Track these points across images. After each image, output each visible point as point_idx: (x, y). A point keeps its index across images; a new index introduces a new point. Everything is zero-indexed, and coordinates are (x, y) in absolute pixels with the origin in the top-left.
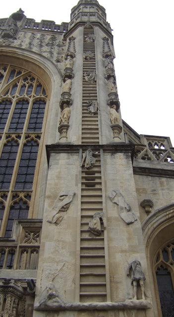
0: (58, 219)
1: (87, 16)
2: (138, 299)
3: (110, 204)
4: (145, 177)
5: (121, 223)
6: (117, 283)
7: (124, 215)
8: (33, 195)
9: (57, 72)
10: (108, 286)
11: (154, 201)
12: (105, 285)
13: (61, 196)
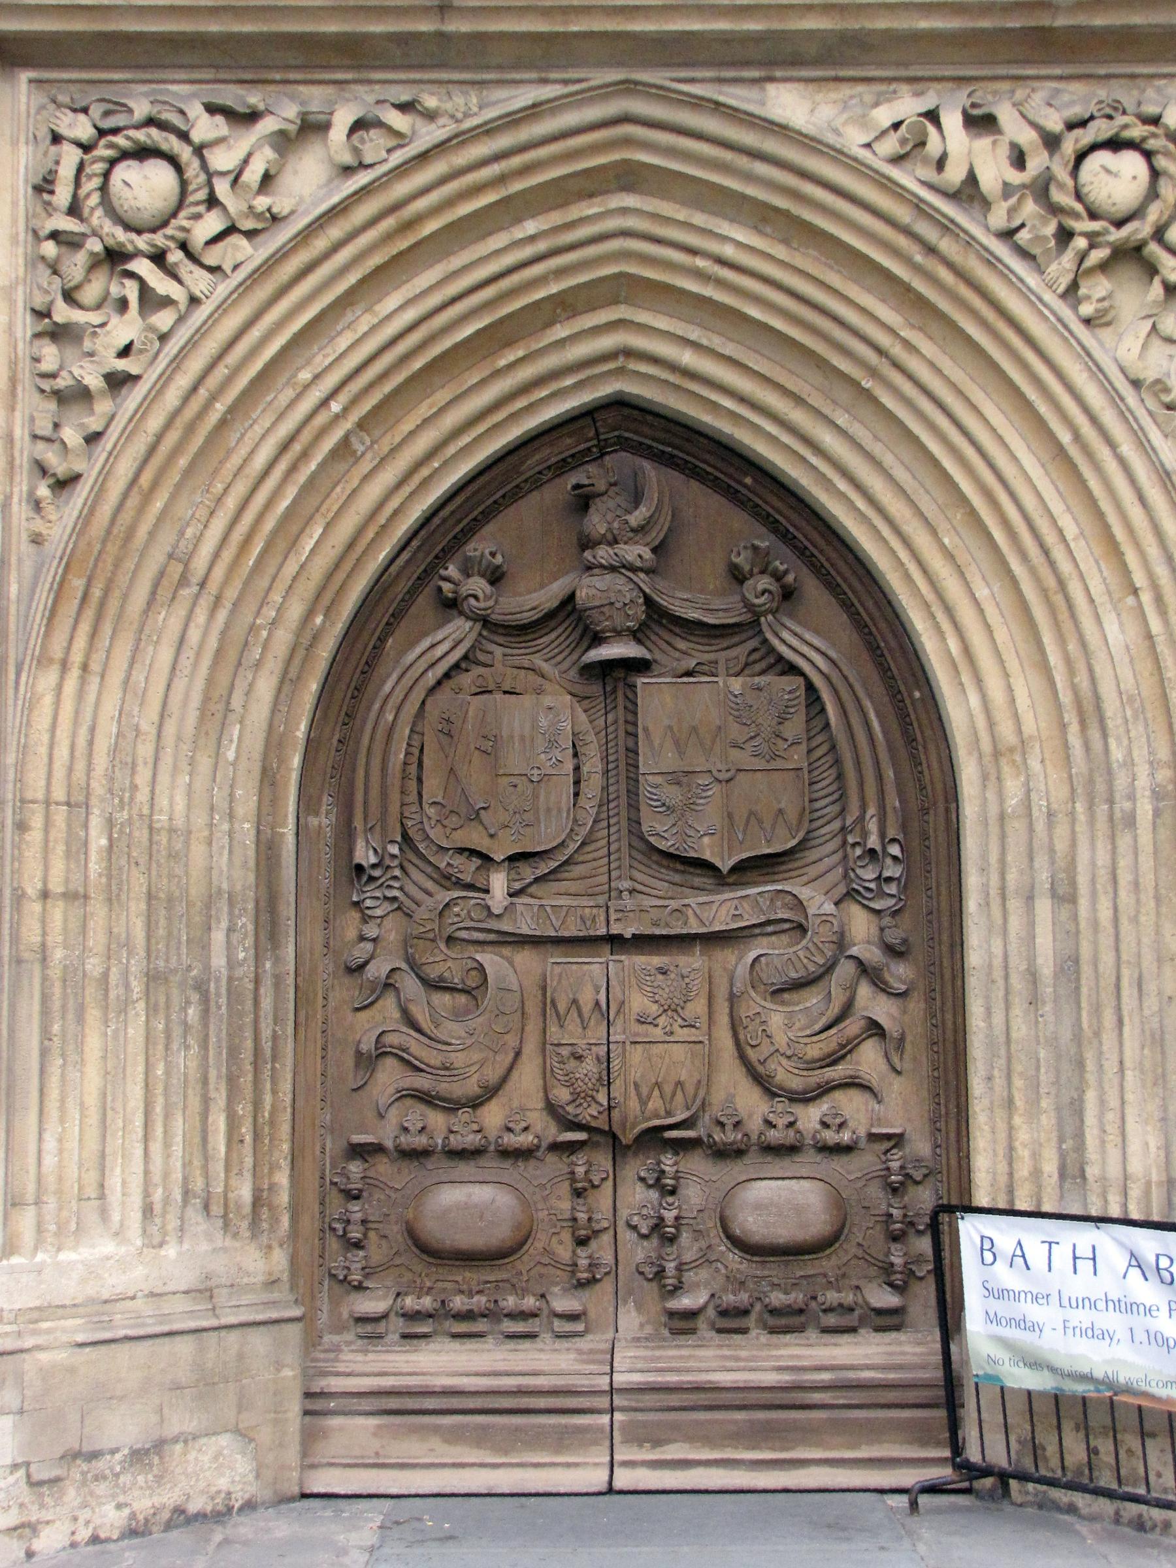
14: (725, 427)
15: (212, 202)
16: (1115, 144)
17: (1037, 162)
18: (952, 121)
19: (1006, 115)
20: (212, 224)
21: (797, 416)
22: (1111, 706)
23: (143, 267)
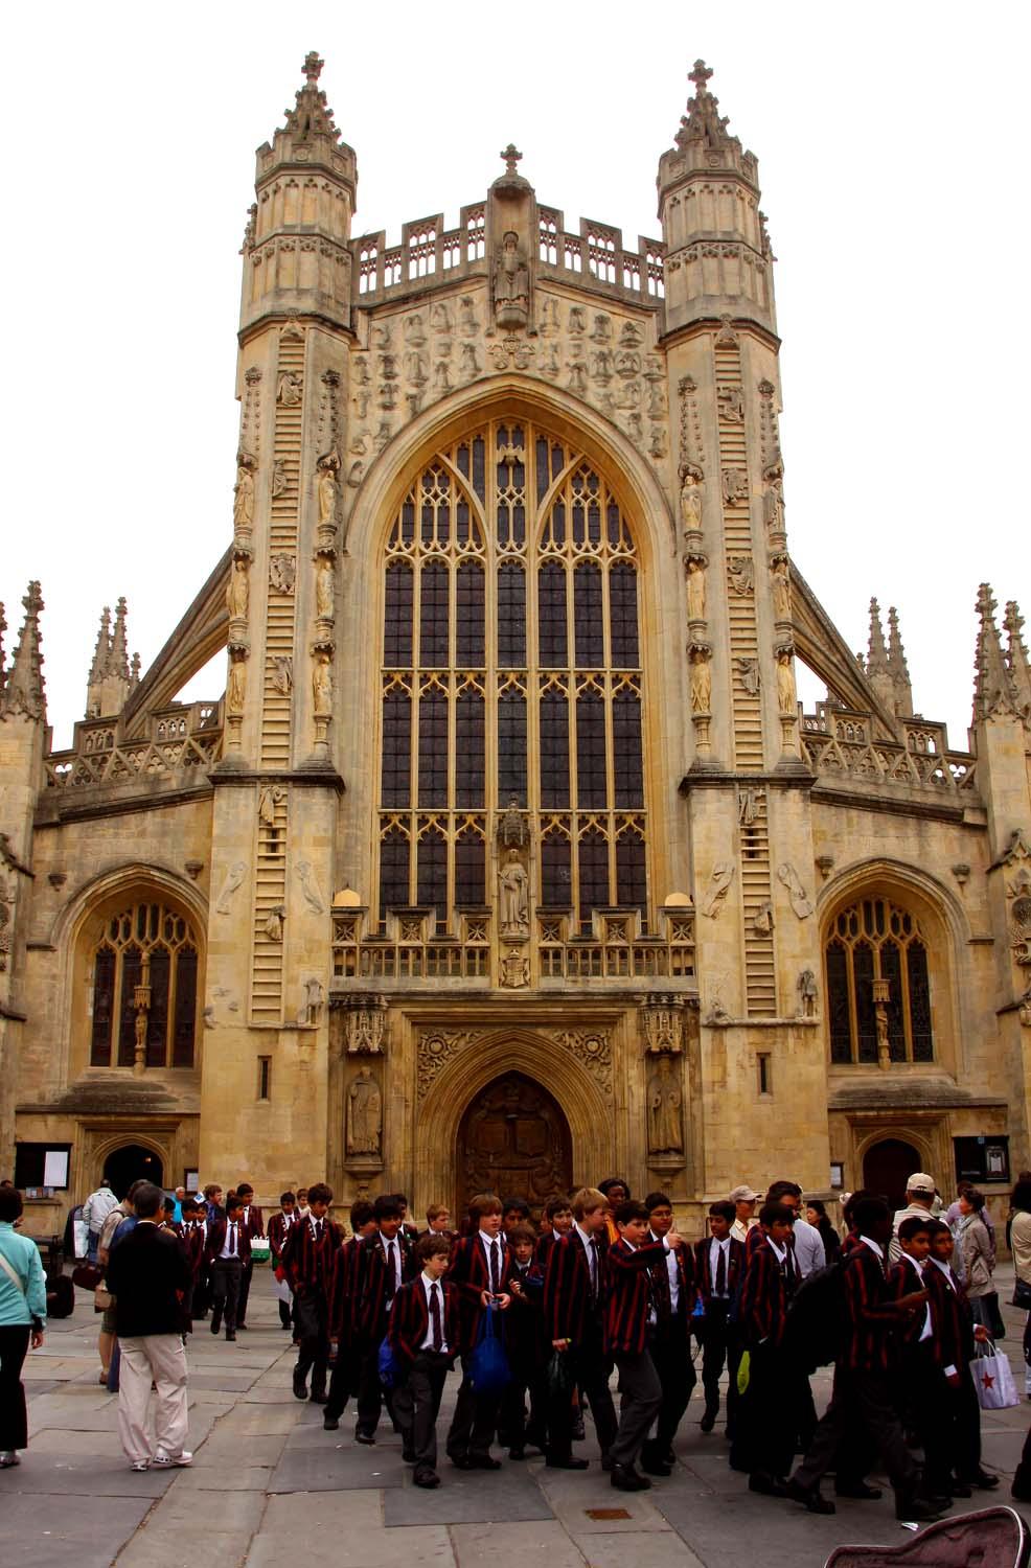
1: (715, 256)
4: (825, 807)
5: (792, 916)
6: (786, 996)
7: (797, 904)
8: (649, 821)
11: (835, 855)
12: (774, 999)
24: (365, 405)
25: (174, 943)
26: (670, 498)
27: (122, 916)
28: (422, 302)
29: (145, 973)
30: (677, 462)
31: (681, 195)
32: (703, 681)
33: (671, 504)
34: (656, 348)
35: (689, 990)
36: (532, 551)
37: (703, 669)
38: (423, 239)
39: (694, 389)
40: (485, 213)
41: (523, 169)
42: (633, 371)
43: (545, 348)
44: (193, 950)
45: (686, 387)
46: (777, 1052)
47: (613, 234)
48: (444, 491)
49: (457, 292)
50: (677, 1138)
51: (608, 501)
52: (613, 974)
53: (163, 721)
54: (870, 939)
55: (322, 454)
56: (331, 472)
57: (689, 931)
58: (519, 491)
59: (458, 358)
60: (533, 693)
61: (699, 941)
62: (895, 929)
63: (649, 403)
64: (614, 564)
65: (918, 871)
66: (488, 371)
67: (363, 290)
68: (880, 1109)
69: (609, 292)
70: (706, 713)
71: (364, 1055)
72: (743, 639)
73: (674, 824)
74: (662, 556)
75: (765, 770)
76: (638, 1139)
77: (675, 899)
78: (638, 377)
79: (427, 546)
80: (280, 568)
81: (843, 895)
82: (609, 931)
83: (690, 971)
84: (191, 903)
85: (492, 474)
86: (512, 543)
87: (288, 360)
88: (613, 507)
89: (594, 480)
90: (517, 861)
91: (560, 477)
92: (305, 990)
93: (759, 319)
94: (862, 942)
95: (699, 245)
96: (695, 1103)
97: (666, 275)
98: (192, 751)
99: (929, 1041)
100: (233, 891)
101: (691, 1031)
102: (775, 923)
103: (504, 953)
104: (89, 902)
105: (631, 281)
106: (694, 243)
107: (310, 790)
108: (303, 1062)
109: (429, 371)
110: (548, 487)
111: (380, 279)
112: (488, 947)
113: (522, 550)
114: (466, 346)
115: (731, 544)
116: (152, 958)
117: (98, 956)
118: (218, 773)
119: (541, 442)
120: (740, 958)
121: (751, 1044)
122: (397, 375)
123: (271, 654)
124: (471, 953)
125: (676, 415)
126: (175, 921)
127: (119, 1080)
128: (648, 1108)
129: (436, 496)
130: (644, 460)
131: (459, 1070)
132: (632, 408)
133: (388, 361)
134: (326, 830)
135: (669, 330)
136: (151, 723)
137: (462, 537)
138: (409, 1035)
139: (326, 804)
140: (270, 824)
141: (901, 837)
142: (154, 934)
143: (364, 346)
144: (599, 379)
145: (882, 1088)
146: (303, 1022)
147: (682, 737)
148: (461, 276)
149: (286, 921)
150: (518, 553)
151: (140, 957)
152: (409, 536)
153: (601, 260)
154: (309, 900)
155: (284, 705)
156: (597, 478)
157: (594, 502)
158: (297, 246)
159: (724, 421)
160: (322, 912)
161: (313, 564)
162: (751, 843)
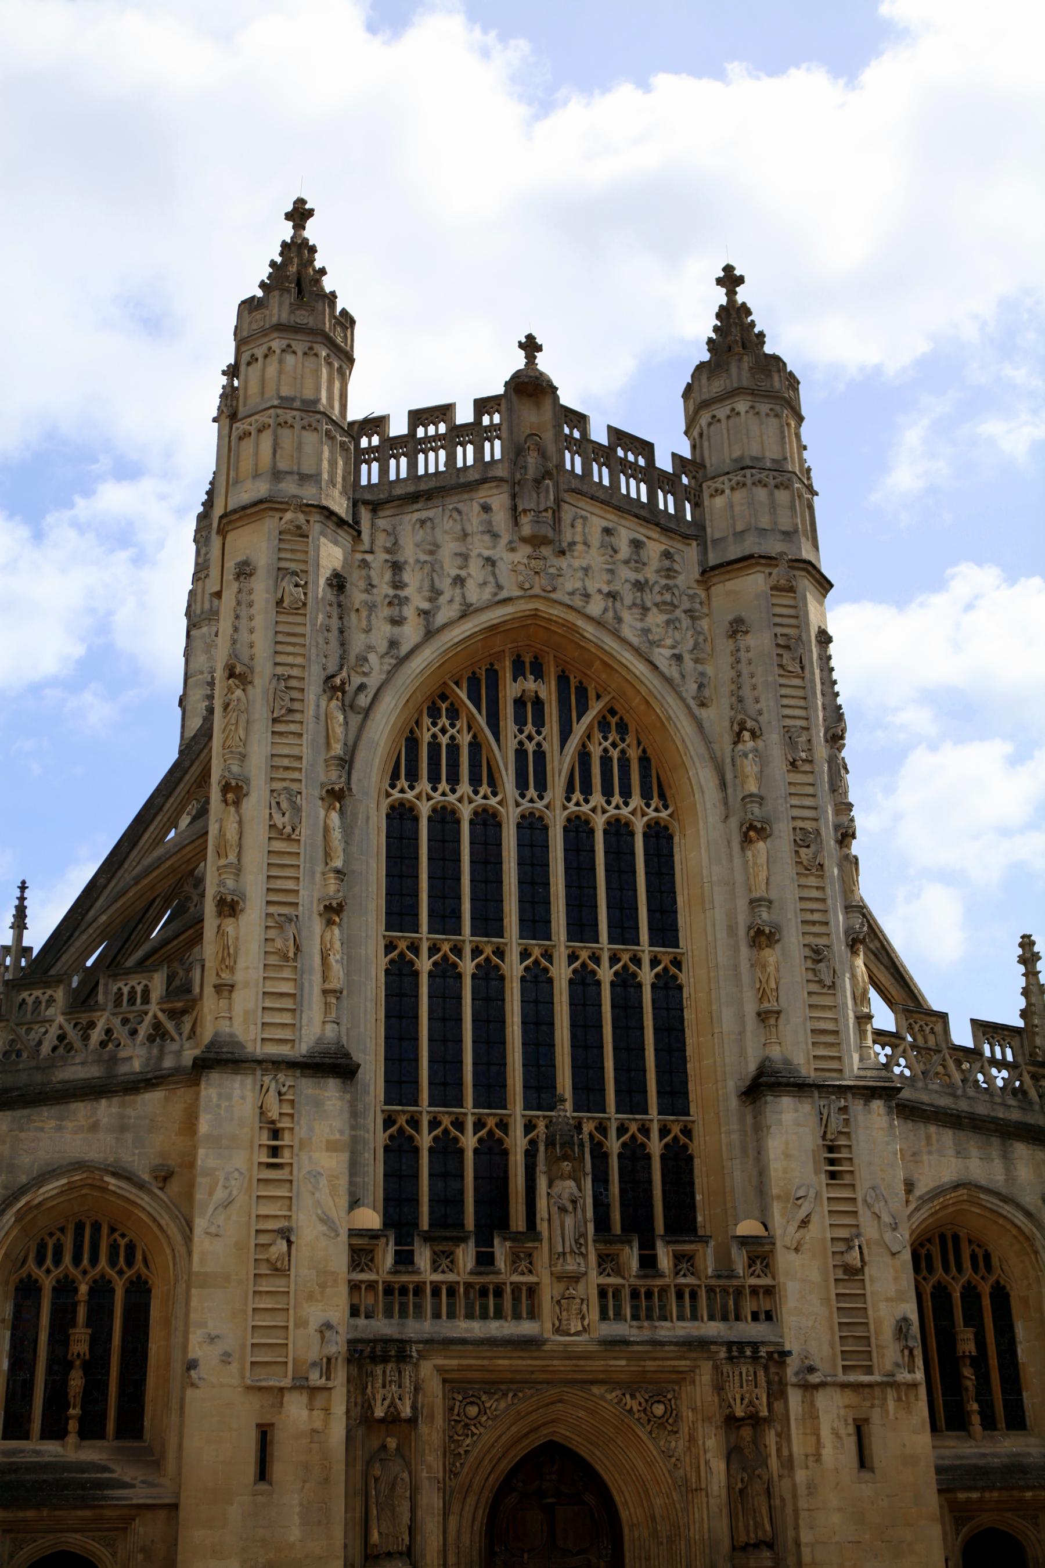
0: (799, 1243)
1: (765, 486)
2: (909, 1372)
3: (869, 1214)
6: (883, 1347)
7: (888, 1236)
8: (698, 1131)
9: (707, 757)
10: (874, 1355)
11: (916, 1176)
13: (798, 1199)
14: (574, 1448)
15: (485, 1413)
16: (658, 1402)
17: (644, 1404)
18: (628, 1396)
19: (638, 1395)
20: (485, 1418)
21: (591, 1447)
22: (657, 1516)
23: (473, 1428)
24: (369, 616)
25: (121, 1273)
26: (718, 754)
27: (51, 1235)
28: (430, 504)
29: (82, 1312)
30: (728, 713)
31: (722, 412)
32: (771, 969)
33: (719, 760)
34: (698, 581)
35: (773, 1339)
36: (558, 804)
37: (771, 956)
38: (431, 430)
39: (746, 632)
40: (503, 407)
41: (544, 363)
42: (672, 604)
43: (575, 570)
44: (146, 1282)
45: (737, 628)
46: (876, 1416)
47: (646, 448)
48: (453, 726)
49: (474, 495)
50: (768, 1528)
51: (640, 751)
52: (681, 1318)
53: (121, 984)
54: (949, 1279)
55: (331, 669)
56: (340, 694)
57: (767, 1266)
58: (539, 733)
59: (475, 571)
60: (561, 973)
61: (782, 1279)
62: (975, 1268)
63: (691, 642)
64: (648, 825)
65: (1005, 1199)
66: (510, 590)
67: (364, 482)
68: (983, 1489)
69: (643, 513)
70: (773, 1005)
71: (392, 1420)
72: (814, 923)
73: (735, 1137)
74: (710, 820)
75: (847, 1073)
76: (722, 1528)
77: (748, 1227)
78: (678, 613)
79: (435, 789)
80: (285, 805)
81: (923, 1226)
82: (676, 1266)
83: (769, 1317)
84: (155, 1220)
85: (508, 711)
86: (532, 792)
87: (289, 556)
88: (645, 761)
89: (623, 728)
90: (570, 1177)
91: (587, 719)
92: (318, 1336)
93: (814, 561)
94: (939, 1282)
95: (748, 472)
96: (786, 1483)
97: (706, 503)
98: (157, 1025)
99: (1020, 1403)
100: (226, 1207)
101: (777, 1392)
102: (867, 1258)
103: (558, 1289)
104: (20, 1217)
105: (666, 503)
106: (743, 469)
107: (323, 1080)
108: (314, 1431)
109: (445, 584)
110: (570, 731)
111: (384, 471)
112: (537, 1284)
113: (545, 802)
114: (488, 559)
115: (797, 812)
116: (92, 1291)
117: (17, 1289)
118: (206, 1055)
119: (563, 680)
120: (828, 1300)
121: (846, 1407)
122: (406, 585)
123: (272, 909)
124: (516, 1287)
125: (724, 660)
126: (122, 1242)
127: (47, 1459)
128: (730, 1488)
129: (443, 731)
130: (688, 707)
131: (496, 1441)
132: (673, 647)
133: (397, 567)
134: (341, 1132)
135: (711, 563)
136: (106, 985)
137: (475, 782)
138: (441, 1396)
139: (341, 1098)
140: (273, 1122)
141: (986, 1159)
142: (94, 1260)
143: (366, 546)
144: (635, 610)
145: (981, 1462)
146: (315, 1378)
147: (742, 1032)
148: (477, 477)
149: (294, 1248)
150: (540, 805)
151: (76, 1290)
152: (413, 777)
153: (632, 476)
154: (322, 1220)
155: (287, 973)
156: (626, 725)
157: (623, 752)
158: (298, 426)
159: (782, 672)
160: (338, 1235)
161: (320, 803)
162: (832, 1162)
